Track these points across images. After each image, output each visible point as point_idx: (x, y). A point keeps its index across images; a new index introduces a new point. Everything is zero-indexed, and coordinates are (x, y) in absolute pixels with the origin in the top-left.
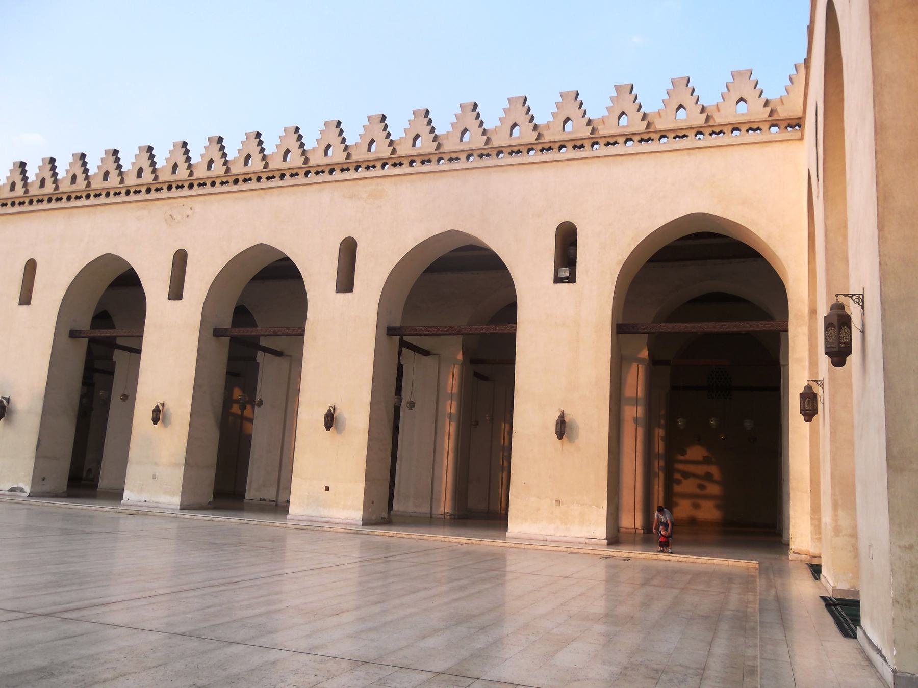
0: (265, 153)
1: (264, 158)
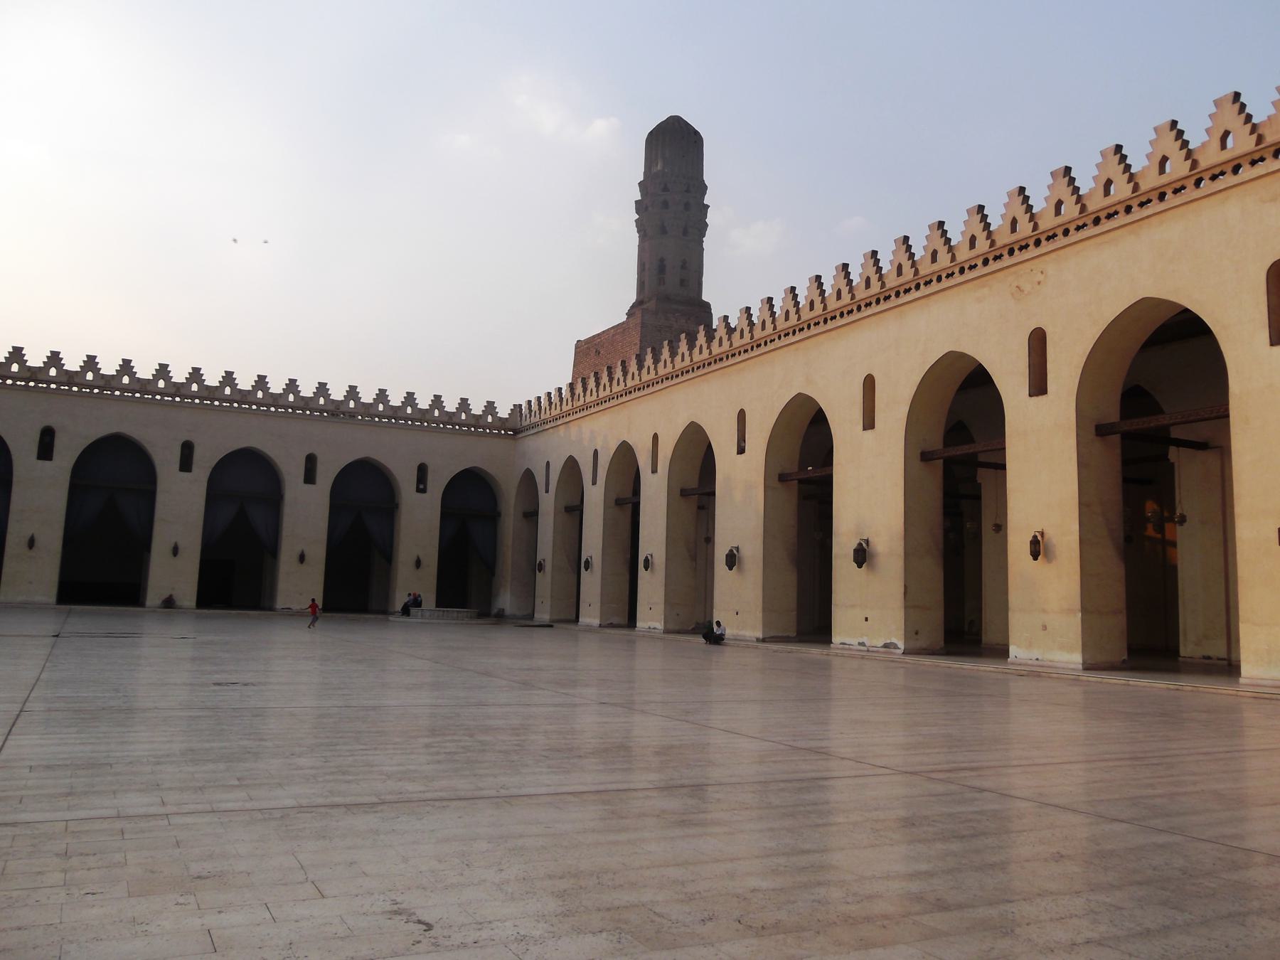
0: (1133, 171)
1: (1131, 178)
